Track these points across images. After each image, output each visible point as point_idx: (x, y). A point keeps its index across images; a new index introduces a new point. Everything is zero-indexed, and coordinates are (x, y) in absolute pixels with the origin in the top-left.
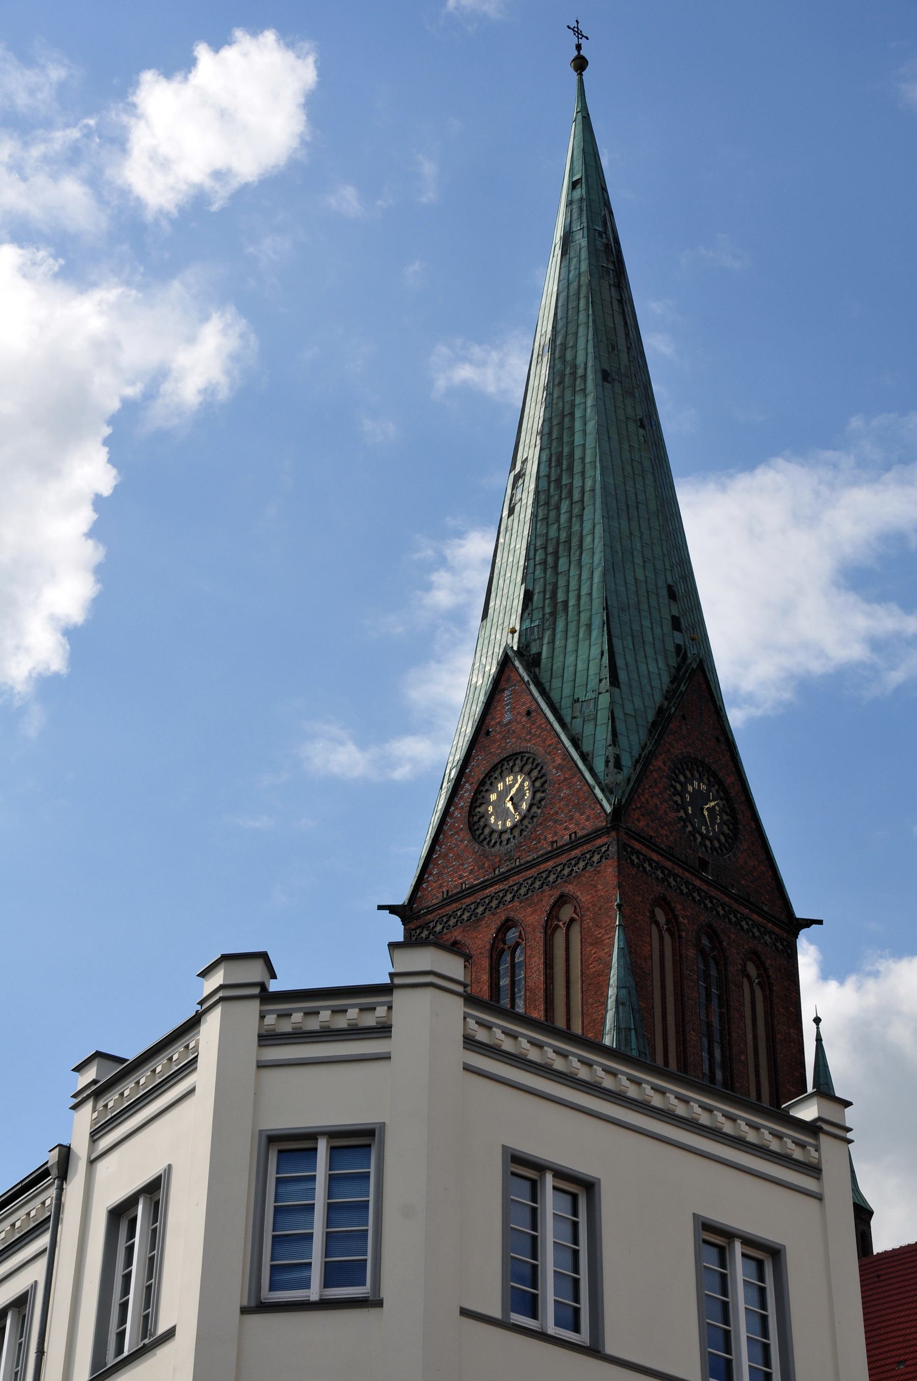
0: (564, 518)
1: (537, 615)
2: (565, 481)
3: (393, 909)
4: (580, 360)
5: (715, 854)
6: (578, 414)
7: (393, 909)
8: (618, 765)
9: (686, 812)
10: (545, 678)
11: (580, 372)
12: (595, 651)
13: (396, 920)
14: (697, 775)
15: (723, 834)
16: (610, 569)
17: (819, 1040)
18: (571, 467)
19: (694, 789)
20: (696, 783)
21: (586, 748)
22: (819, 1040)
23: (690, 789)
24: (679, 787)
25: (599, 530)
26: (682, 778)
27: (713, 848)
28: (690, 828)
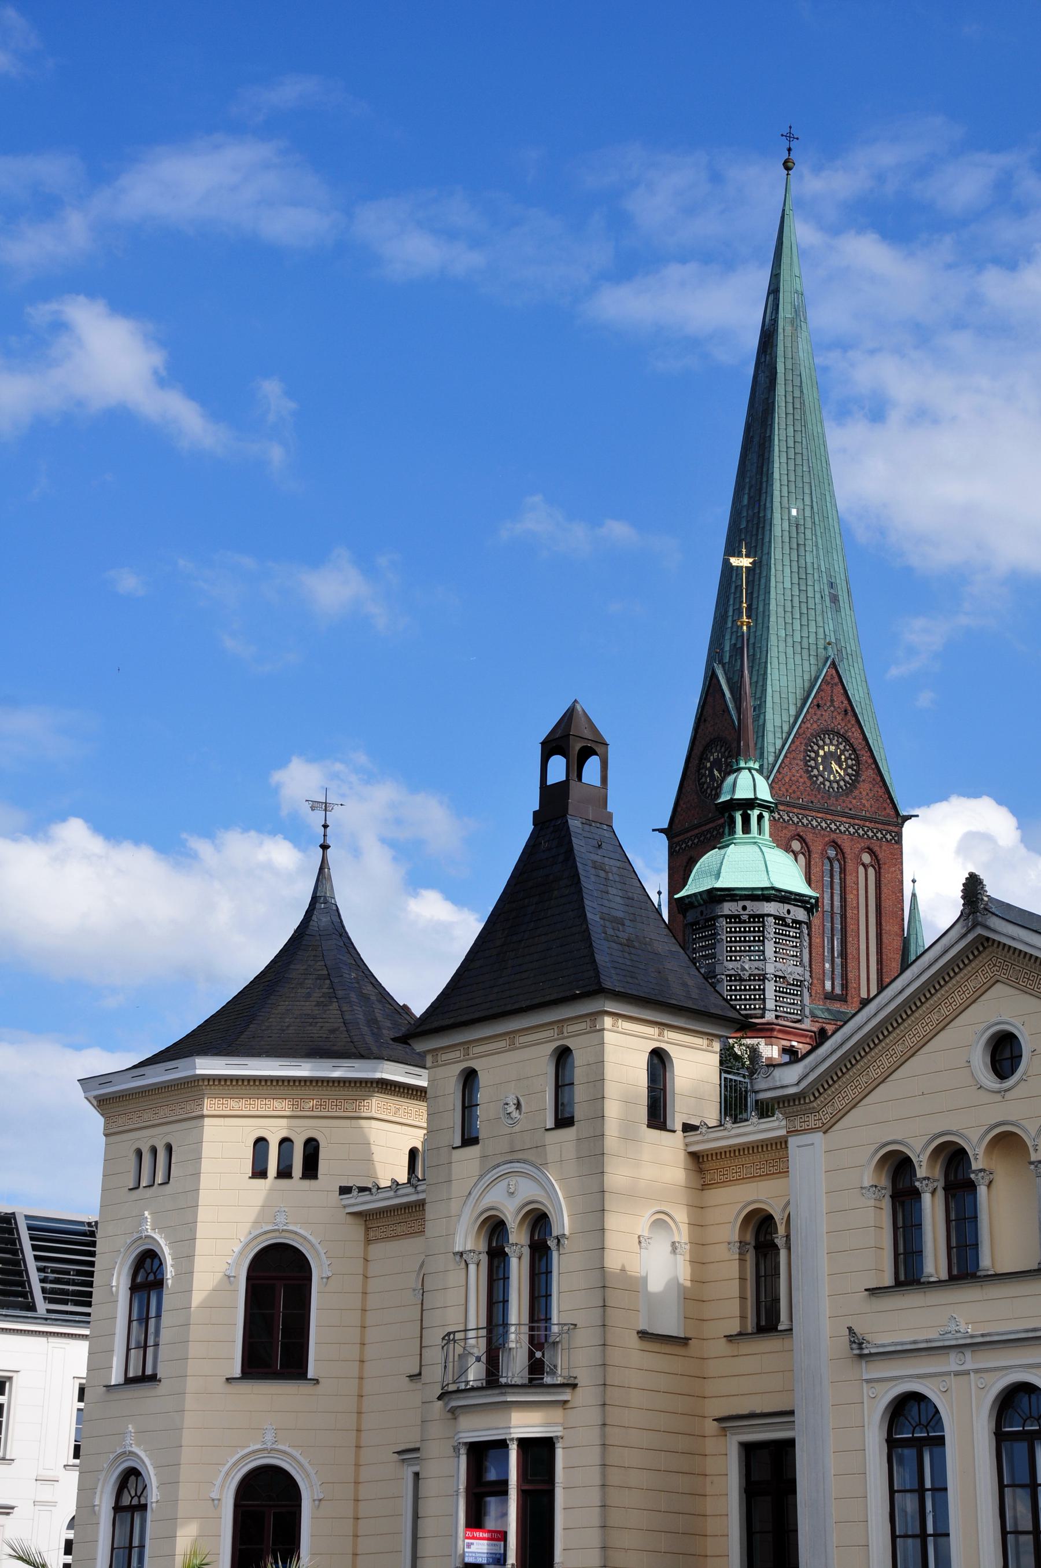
3: (661, 831)
5: (841, 790)
7: (661, 831)
9: (818, 770)
13: (663, 836)
14: (827, 741)
15: (848, 775)
17: (914, 895)
19: (825, 752)
20: (826, 748)
22: (914, 895)
23: (821, 753)
24: (813, 755)
26: (816, 748)
27: (839, 787)
28: (821, 779)
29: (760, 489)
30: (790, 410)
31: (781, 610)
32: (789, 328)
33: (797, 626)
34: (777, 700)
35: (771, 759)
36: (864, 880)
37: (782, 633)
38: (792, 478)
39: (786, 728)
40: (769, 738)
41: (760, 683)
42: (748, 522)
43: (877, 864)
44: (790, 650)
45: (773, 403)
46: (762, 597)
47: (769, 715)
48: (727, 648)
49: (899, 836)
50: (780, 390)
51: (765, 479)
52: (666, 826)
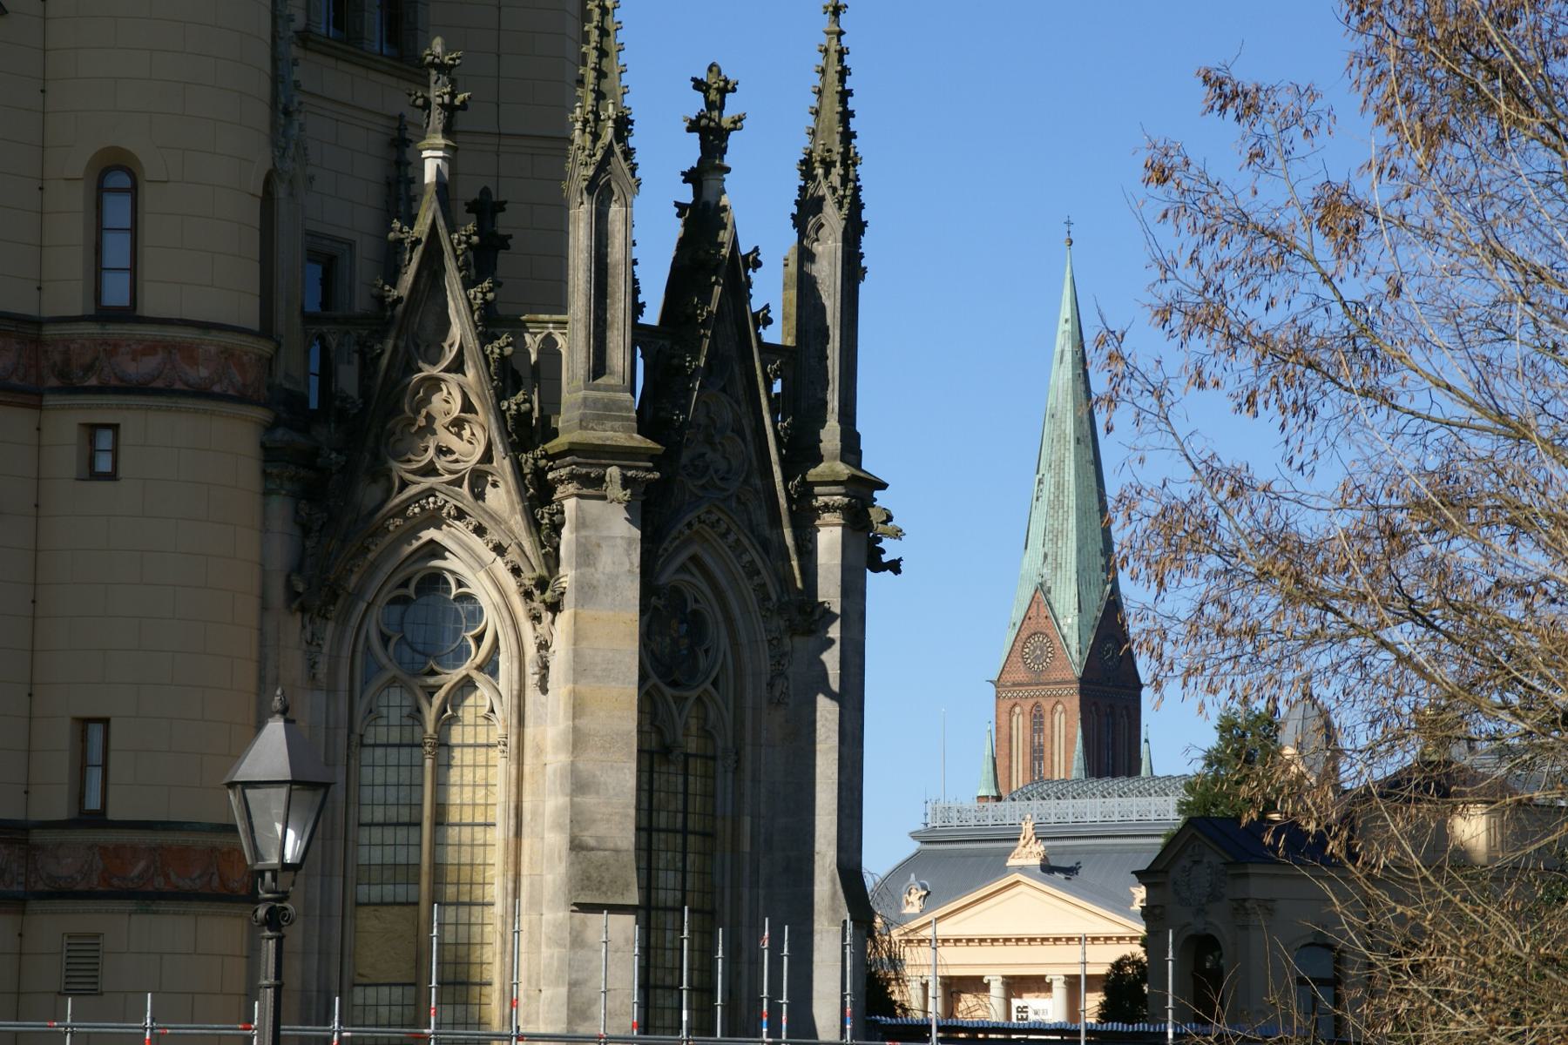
0: (1061, 518)
1: (1050, 567)
2: (1061, 499)
4: (1067, 432)
6: (1067, 462)
8: (1080, 653)
10: (1052, 601)
11: (1068, 439)
12: (1072, 595)
16: (1079, 551)
18: (1063, 492)
21: (1068, 641)
25: (1075, 529)
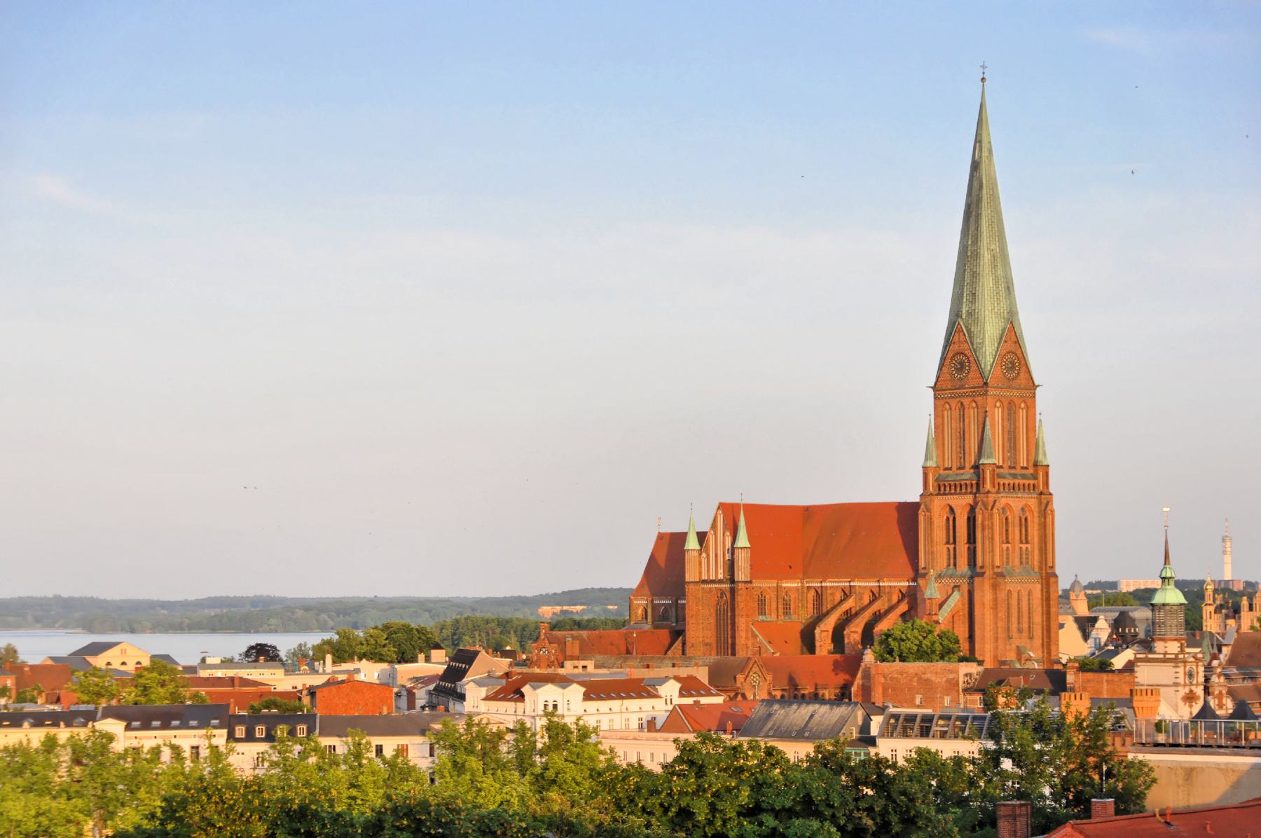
29: (977, 238)
30: (989, 201)
31: (989, 298)
32: (986, 161)
33: (996, 305)
34: (989, 340)
35: (989, 368)
36: (1022, 414)
37: (990, 308)
38: (991, 234)
39: (994, 353)
40: (988, 358)
41: (982, 332)
42: (972, 253)
43: (1027, 408)
44: (993, 316)
45: (982, 198)
46: (980, 291)
47: (987, 348)
48: (964, 311)
49: (1034, 394)
50: (984, 192)
51: (979, 234)
52: (932, 385)
